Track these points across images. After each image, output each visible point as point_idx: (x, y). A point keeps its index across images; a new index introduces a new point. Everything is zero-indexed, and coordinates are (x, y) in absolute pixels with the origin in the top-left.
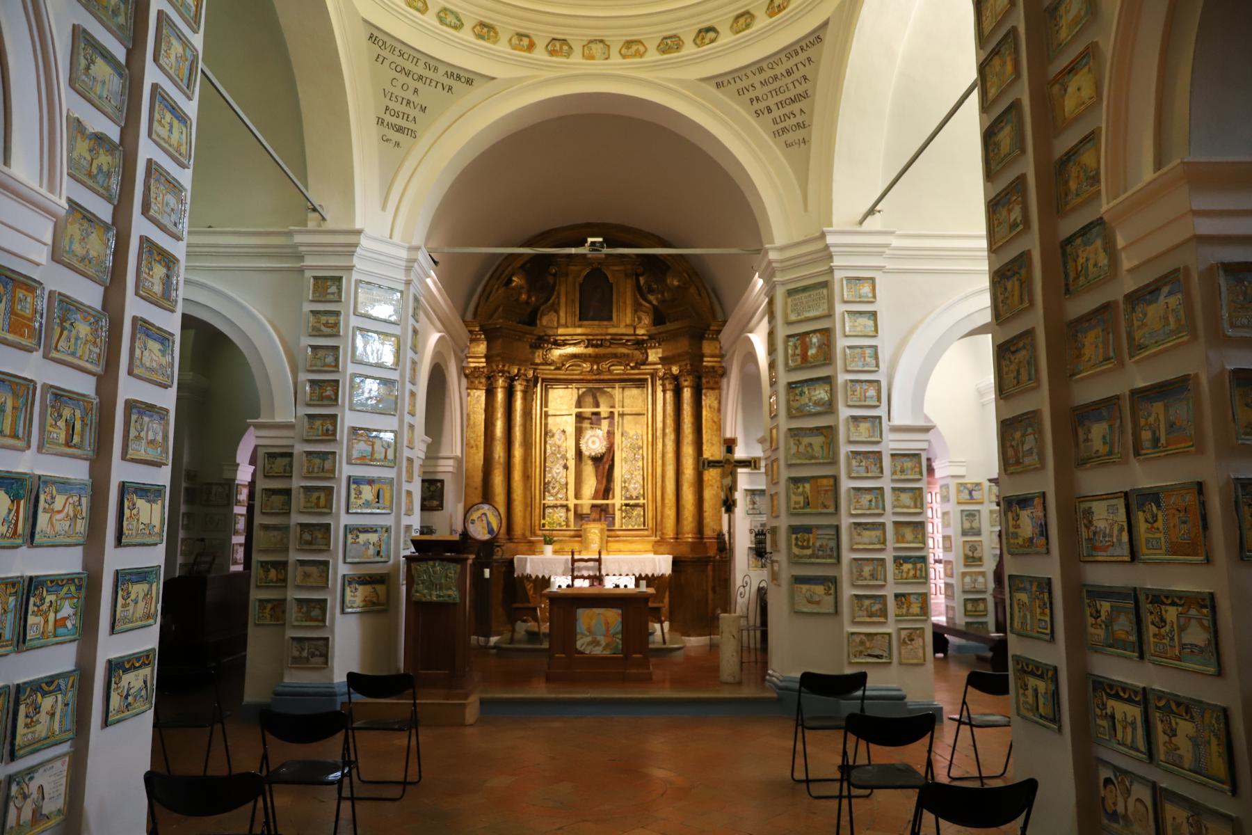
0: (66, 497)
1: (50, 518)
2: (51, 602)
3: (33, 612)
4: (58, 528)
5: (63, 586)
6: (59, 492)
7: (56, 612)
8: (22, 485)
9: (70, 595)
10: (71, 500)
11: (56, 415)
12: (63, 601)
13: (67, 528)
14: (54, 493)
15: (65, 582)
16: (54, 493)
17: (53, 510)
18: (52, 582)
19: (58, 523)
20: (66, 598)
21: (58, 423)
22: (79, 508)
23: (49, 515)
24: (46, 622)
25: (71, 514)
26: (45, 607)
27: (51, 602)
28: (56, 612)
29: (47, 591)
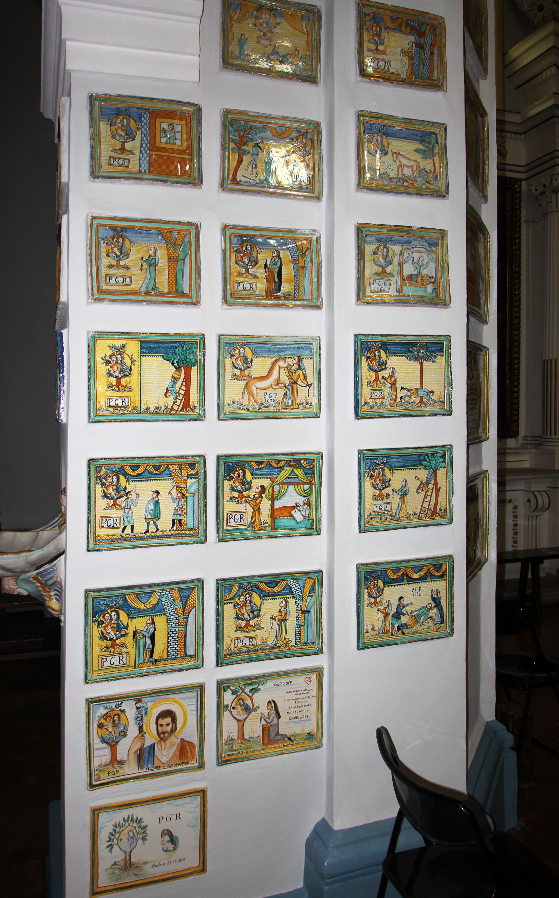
0: (274, 359)
1: (247, 386)
2: (262, 487)
3: (232, 498)
4: (261, 397)
5: (281, 468)
6: (255, 353)
7: (273, 500)
8: (190, 349)
9: (296, 480)
10: (281, 363)
11: (246, 261)
12: (284, 487)
13: (280, 397)
14: (249, 355)
15: (282, 464)
16: (249, 355)
17: (249, 376)
18: (259, 463)
19: (261, 392)
20: (289, 484)
21: (251, 271)
22: (300, 372)
23: (244, 383)
24: (257, 510)
25: (285, 379)
26: (252, 493)
27: (262, 487)
28: (273, 500)
29: (252, 474)
